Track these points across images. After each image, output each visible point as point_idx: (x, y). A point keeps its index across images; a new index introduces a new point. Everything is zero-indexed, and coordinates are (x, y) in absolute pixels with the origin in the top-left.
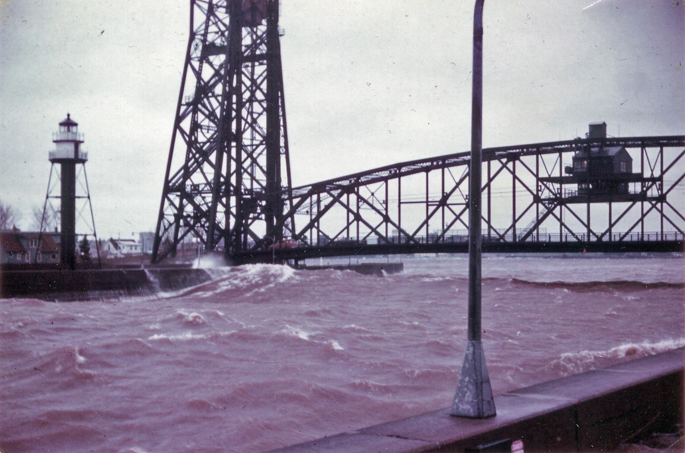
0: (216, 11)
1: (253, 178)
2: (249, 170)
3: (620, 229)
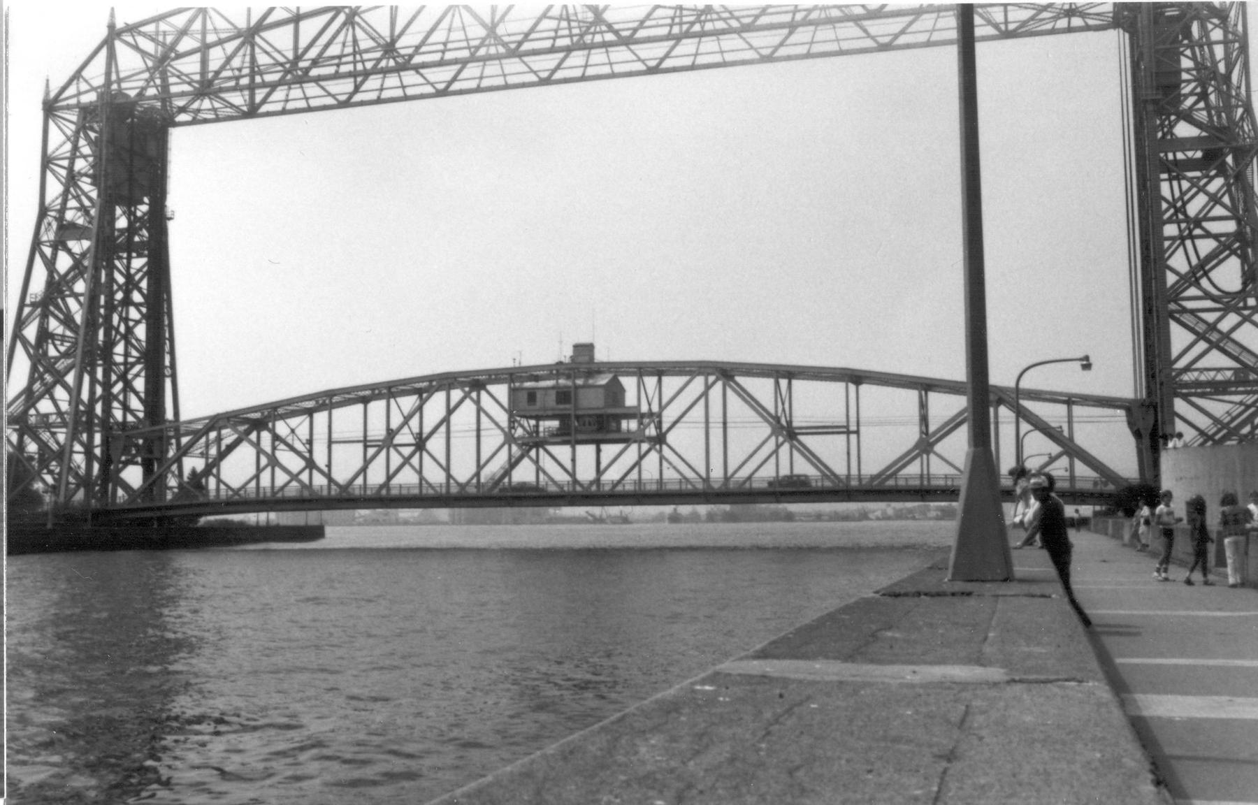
0: (79, 180)
1: (126, 408)
2: (121, 397)
3: (612, 475)
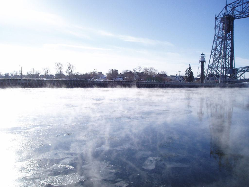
1: (228, 66)
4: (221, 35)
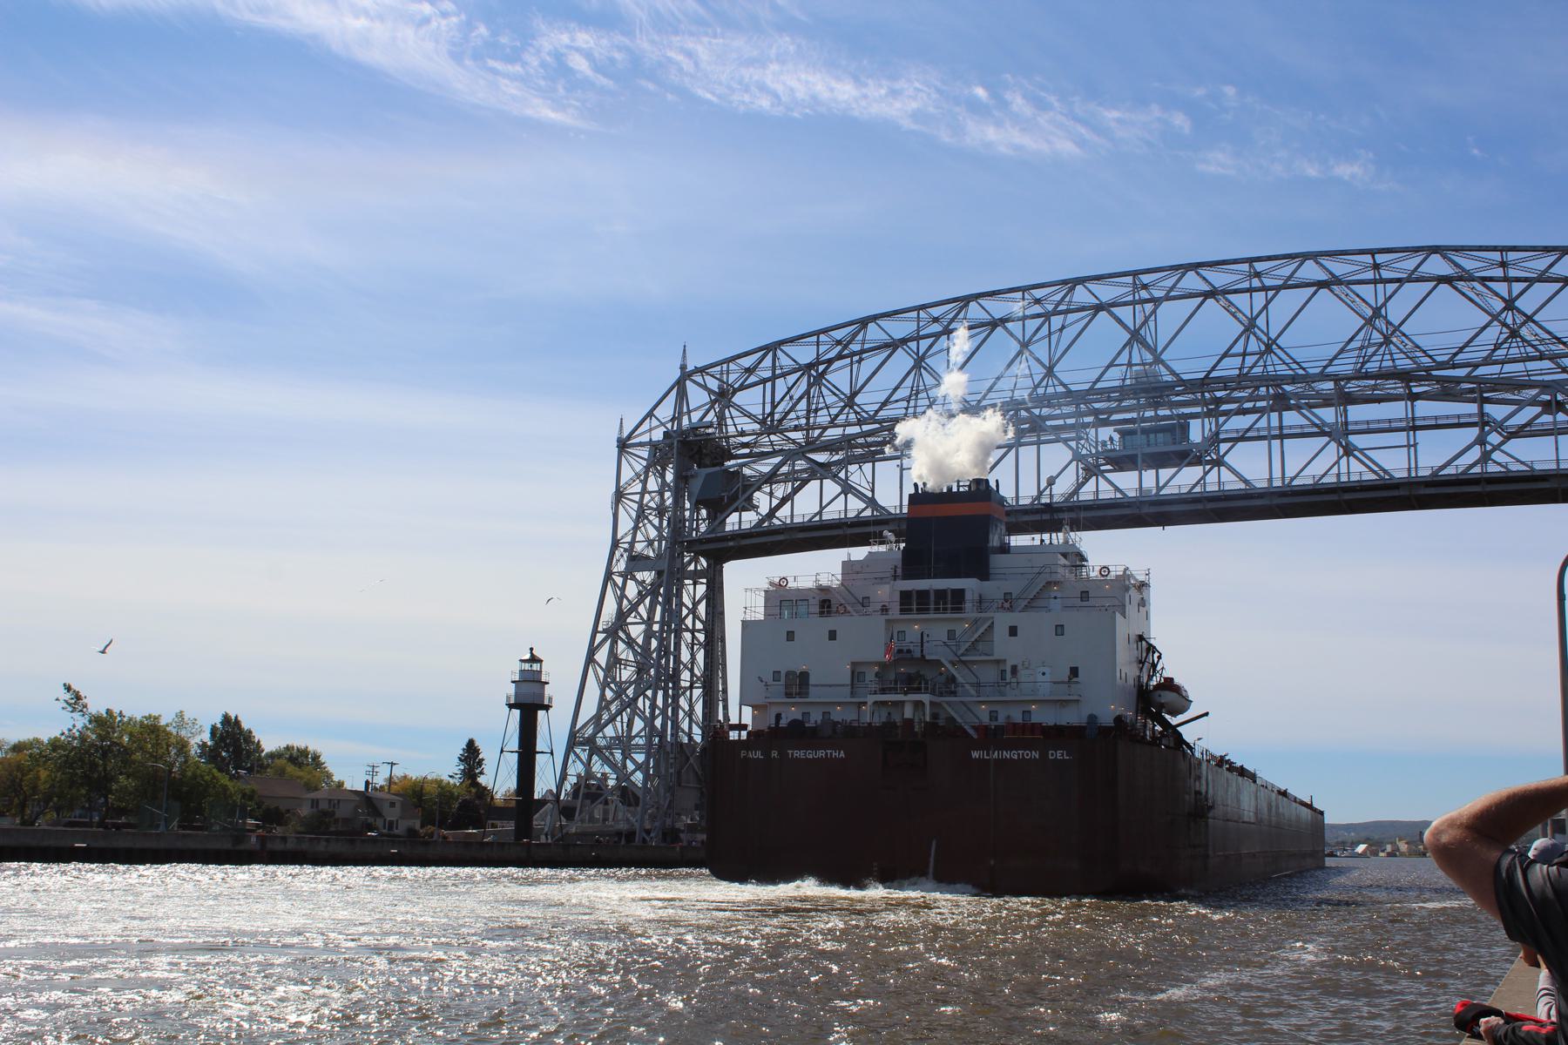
4: (650, 543)
